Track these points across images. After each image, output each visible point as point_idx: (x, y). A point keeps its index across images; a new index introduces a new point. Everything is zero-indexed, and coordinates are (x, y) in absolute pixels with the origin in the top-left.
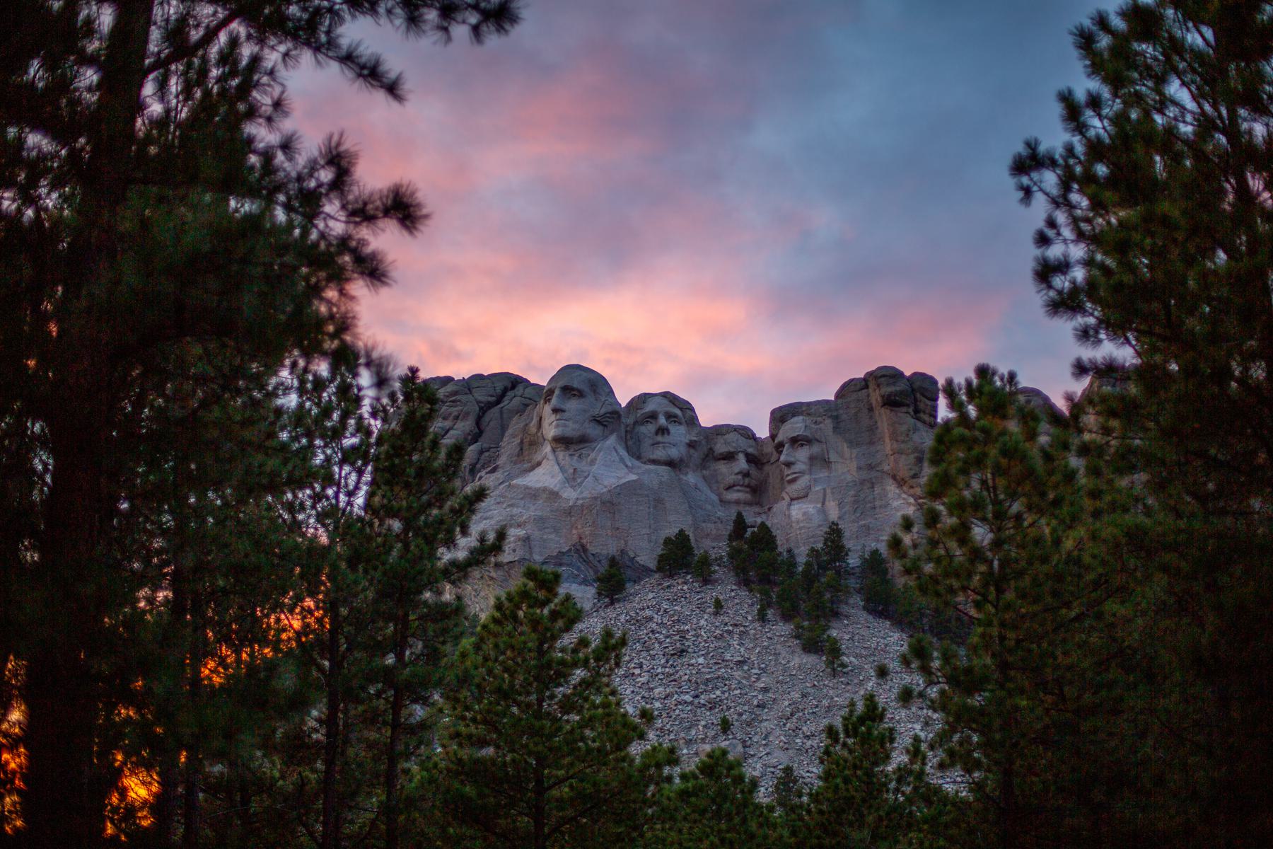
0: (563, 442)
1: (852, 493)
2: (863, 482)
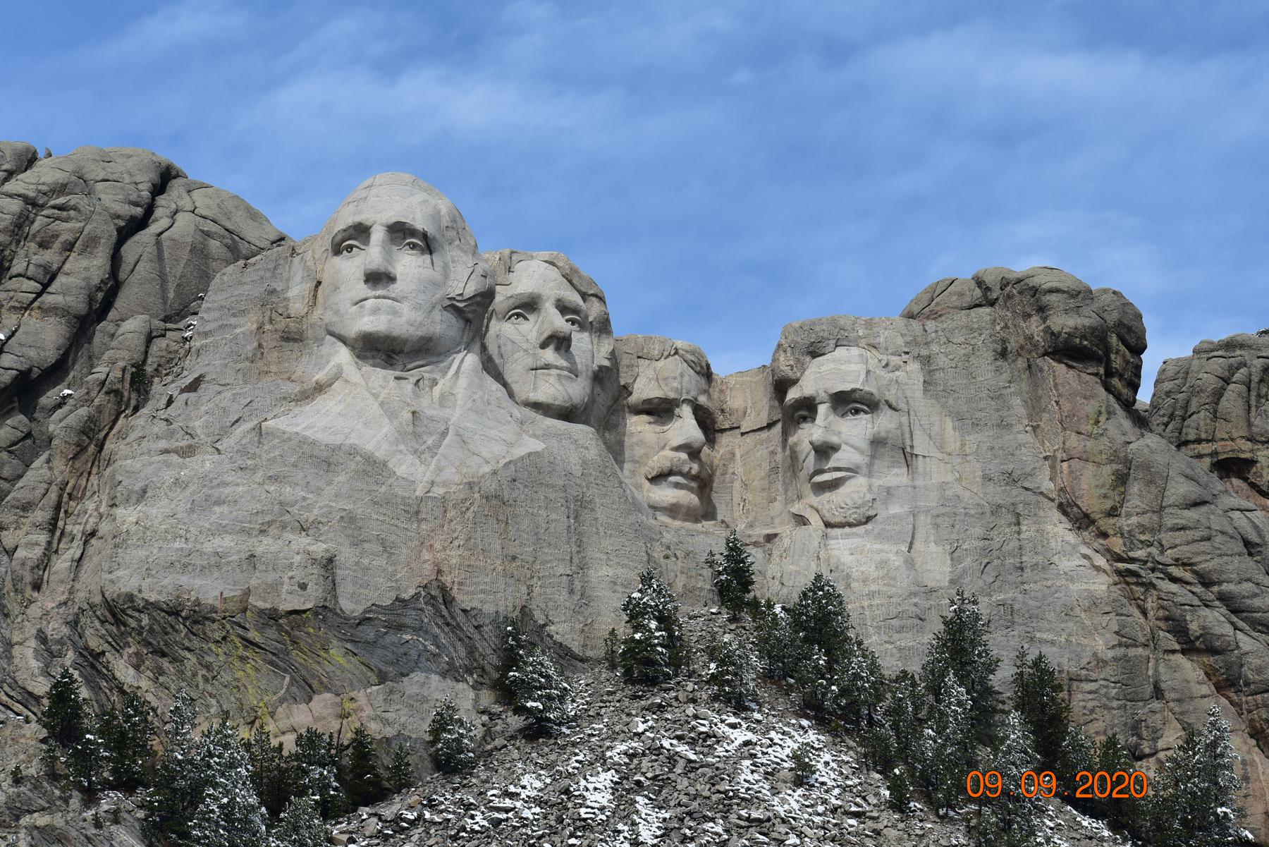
0: (380, 350)
1: (978, 531)
2: (996, 509)
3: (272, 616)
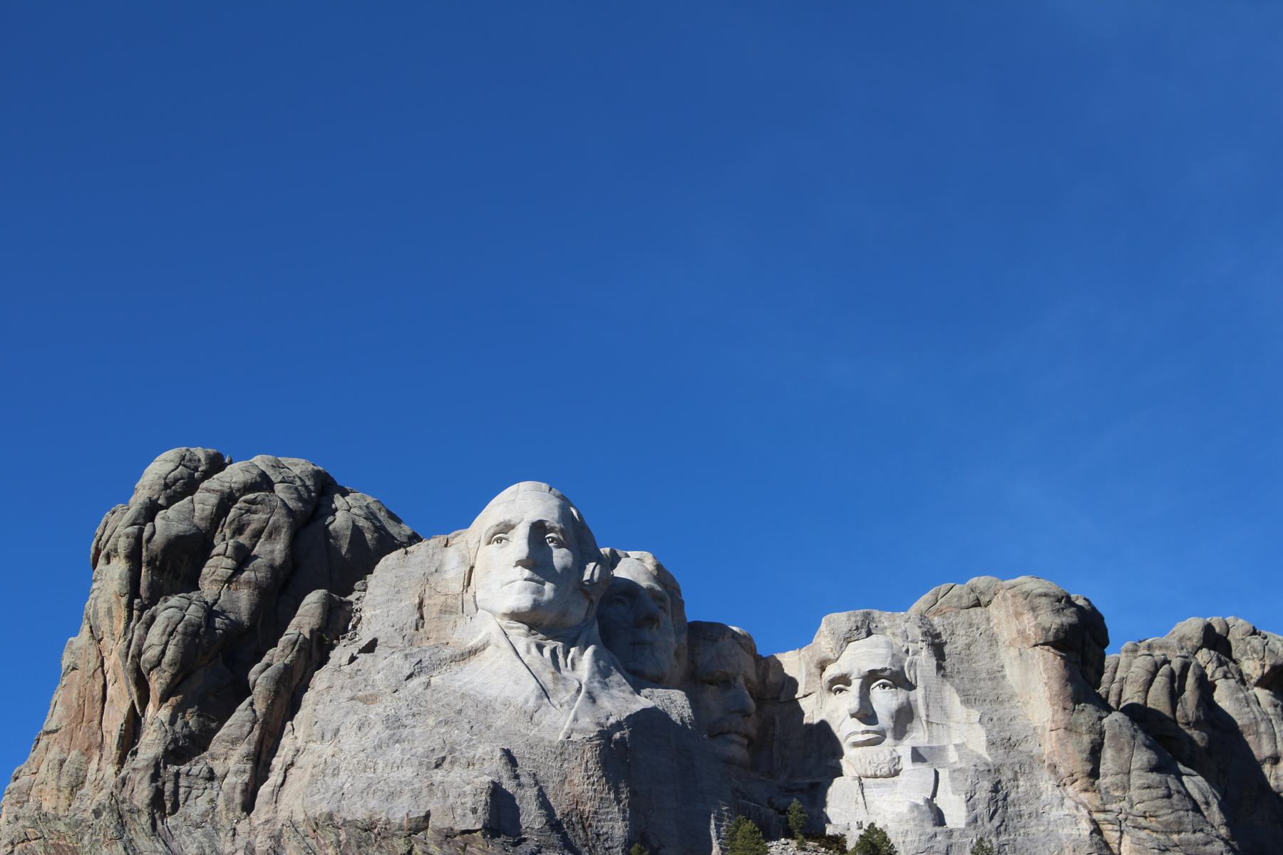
1: (986, 785)
3: (449, 835)
